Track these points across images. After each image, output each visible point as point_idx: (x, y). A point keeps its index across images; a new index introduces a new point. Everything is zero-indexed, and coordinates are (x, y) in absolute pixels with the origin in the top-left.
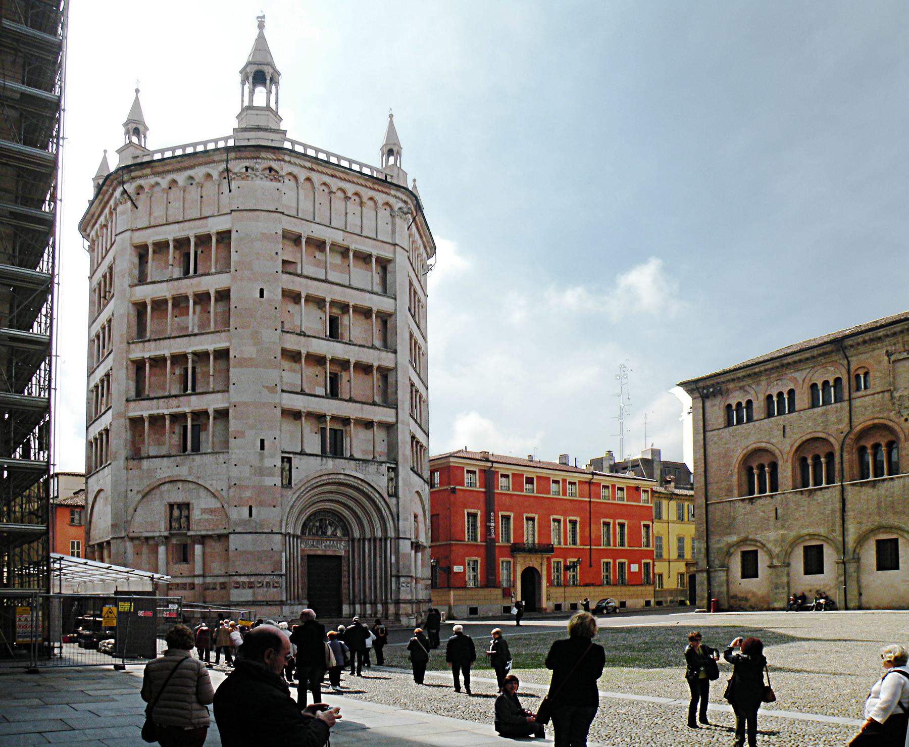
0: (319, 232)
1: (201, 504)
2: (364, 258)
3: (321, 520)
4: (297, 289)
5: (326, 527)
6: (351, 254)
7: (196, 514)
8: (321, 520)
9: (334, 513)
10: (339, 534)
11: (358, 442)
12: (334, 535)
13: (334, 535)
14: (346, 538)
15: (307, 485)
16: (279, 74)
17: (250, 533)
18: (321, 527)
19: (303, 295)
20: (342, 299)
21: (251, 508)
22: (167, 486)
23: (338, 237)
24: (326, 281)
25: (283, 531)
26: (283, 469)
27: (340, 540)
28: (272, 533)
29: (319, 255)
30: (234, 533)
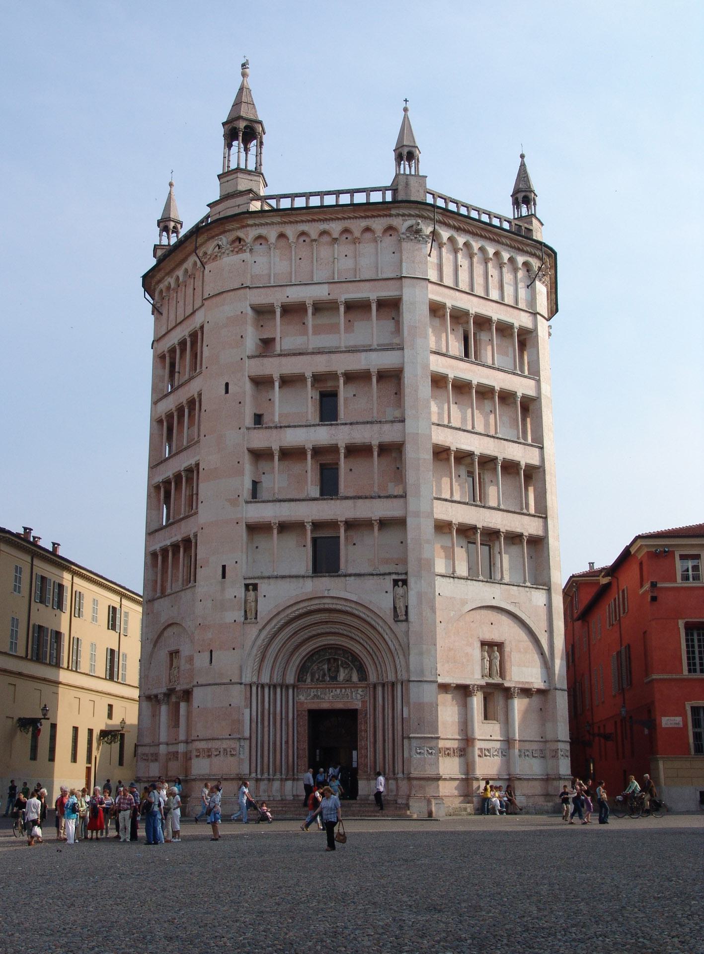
0: (295, 295)
3: (329, 660)
4: (267, 372)
5: (338, 671)
9: (346, 651)
10: (355, 678)
11: (354, 554)
12: (349, 680)
13: (349, 680)
18: (329, 670)
20: (328, 369)
21: (211, 651)
22: (169, 629)
23: (321, 293)
27: (356, 687)
28: (231, 683)
30: (198, 685)
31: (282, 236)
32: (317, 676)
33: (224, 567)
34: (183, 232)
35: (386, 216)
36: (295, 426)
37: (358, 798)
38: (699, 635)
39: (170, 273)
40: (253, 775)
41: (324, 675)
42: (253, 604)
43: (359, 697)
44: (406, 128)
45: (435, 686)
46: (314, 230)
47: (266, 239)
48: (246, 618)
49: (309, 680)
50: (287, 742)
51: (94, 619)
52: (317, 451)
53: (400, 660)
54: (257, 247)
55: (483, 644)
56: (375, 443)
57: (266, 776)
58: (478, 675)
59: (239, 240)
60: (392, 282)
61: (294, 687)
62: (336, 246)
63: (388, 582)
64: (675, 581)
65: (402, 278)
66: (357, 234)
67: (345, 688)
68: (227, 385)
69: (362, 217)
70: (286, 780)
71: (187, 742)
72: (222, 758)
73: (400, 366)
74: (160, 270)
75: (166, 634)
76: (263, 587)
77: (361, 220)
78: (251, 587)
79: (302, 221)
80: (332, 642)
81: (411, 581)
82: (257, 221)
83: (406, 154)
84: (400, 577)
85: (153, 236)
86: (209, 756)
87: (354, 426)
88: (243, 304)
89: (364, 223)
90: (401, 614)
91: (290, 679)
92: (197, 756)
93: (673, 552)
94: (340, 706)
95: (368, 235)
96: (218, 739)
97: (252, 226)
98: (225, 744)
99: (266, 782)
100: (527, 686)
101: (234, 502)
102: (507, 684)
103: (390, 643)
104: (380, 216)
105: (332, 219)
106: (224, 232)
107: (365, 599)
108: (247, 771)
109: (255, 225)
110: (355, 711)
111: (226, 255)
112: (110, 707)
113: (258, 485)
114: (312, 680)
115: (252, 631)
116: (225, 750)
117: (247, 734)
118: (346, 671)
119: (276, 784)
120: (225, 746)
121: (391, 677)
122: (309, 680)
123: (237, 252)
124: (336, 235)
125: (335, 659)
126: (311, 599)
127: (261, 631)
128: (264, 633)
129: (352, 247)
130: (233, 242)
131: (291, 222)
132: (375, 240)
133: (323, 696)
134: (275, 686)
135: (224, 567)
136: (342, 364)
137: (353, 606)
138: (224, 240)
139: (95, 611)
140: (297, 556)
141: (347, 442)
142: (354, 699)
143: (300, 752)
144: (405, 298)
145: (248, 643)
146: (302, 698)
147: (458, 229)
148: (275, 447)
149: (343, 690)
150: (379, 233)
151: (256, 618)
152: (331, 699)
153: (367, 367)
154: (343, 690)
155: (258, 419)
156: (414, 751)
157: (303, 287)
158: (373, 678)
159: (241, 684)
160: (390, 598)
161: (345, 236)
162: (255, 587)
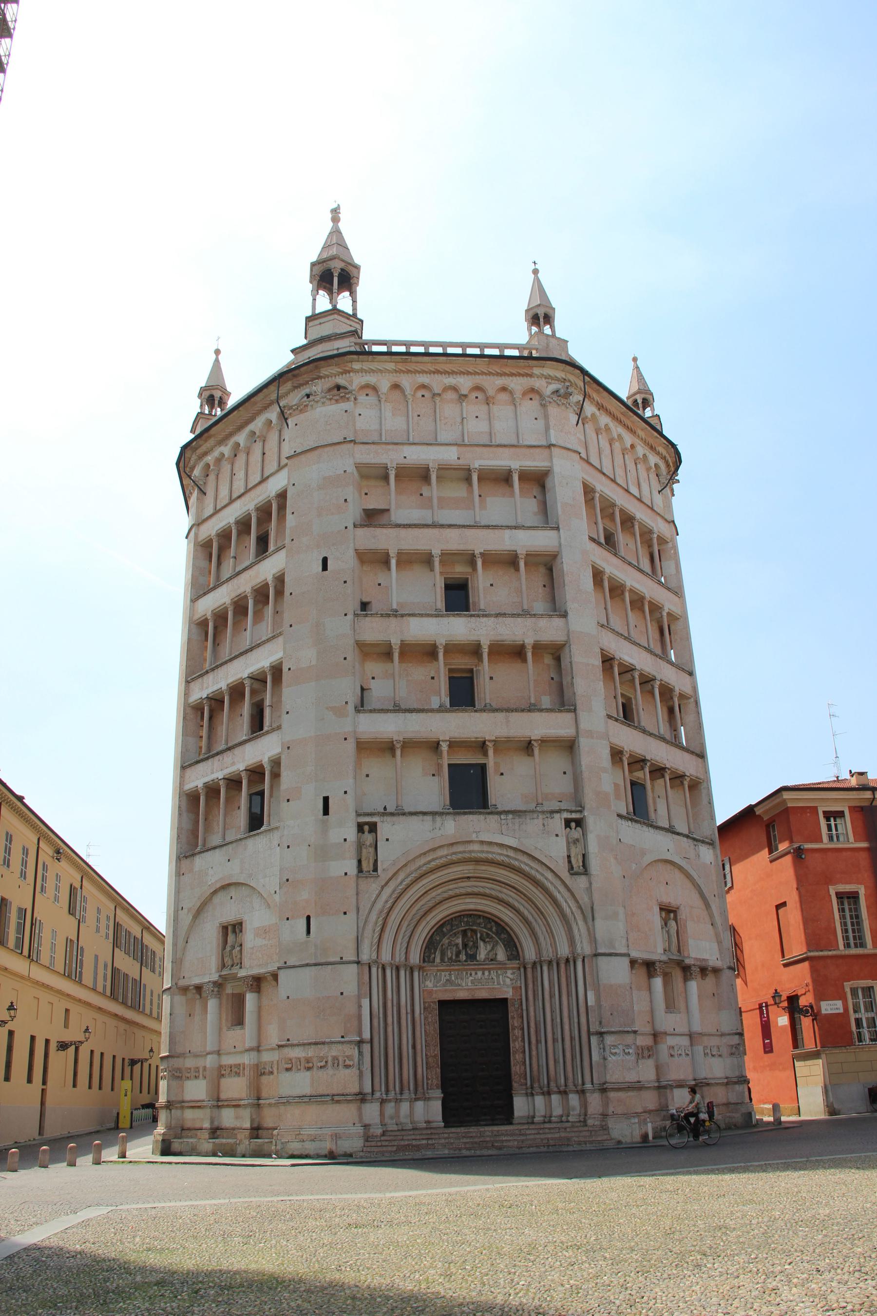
0: (415, 455)
1: (257, 919)
2: (502, 479)
3: (464, 932)
6: (475, 477)
7: (249, 939)
8: (464, 932)
10: (501, 955)
11: (507, 784)
14: (515, 964)
15: (408, 870)
16: (357, 268)
17: (307, 965)
18: (465, 946)
19: (393, 553)
20: (462, 547)
21: (308, 918)
23: (450, 455)
24: (434, 526)
25: (365, 957)
26: (360, 846)
27: (502, 967)
28: (342, 962)
29: (425, 491)
30: (286, 967)
31: (396, 386)
32: (450, 955)
33: (326, 800)
34: (231, 402)
35: (527, 375)
36: (421, 615)
37: (515, 1121)
38: (849, 904)
39: (221, 442)
40: (377, 1095)
41: (458, 954)
42: (372, 850)
43: (508, 980)
44: (538, 288)
45: (626, 961)
46: (437, 382)
47: (375, 389)
48: (360, 870)
49: (438, 960)
50: (414, 1047)
51: (56, 899)
52: (452, 649)
53: (580, 929)
54: (362, 398)
55: (661, 909)
56: (529, 641)
57: (392, 1095)
58: (660, 950)
59: (338, 387)
60: (538, 450)
61: (421, 968)
62: (464, 404)
63: (557, 823)
64: (821, 840)
65: (550, 446)
66: (491, 392)
67: (489, 970)
68: (325, 561)
69: (498, 374)
70: (417, 1099)
71: (218, 1053)
72: (330, 1071)
73: (556, 549)
74: (210, 437)
75: (216, 900)
76: (385, 828)
77: (496, 377)
78: (366, 828)
79: (423, 372)
80: (472, 907)
81: (591, 821)
82: (366, 366)
83: (540, 316)
84: (574, 816)
85: (194, 406)
86: (309, 1069)
87: (501, 619)
88: (343, 462)
89: (500, 382)
90: (581, 867)
91: (415, 958)
92: (287, 1070)
93: (816, 808)
94: (483, 994)
95: (503, 396)
96: (323, 1043)
97: (356, 371)
98: (335, 1051)
99: (393, 1104)
100: (704, 964)
101: (339, 712)
102: (687, 961)
103: (564, 905)
104: (520, 375)
105: (462, 373)
106: (319, 378)
107: (528, 845)
108: (368, 1089)
109: (362, 370)
110: (506, 1000)
111: (320, 404)
112: (67, 1011)
113: (365, 693)
114: (442, 960)
115: (372, 887)
116: (335, 1058)
117: (366, 1035)
118: (489, 947)
119: (405, 1107)
120: (334, 1053)
121: (564, 951)
122: (438, 960)
123: (337, 401)
124: (464, 392)
125: (472, 930)
126: (452, 844)
127: (383, 887)
128: (388, 891)
129: (484, 408)
130: (330, 390)
131: (409, 372)
132: (513, 402)
133: (459, 981)
134: (398, 969)
135: (326, 800)
136: (480, 542)
137: (511, 853)
138: (318, 387)
139: (57, 888)
140: (428, 787)
141: (493, 638)
142: (502, 984)
143: (430, 1060)
144: (557, 469)
145: (365, 905)
146: (429, 984)
147: (600, 407)
148: (395, 642)
149: (487, 973)
150: (518, 395)
151: (375, 869)
152: (470, 985)
153: (513, 548)
155: (364, 606)
156: (607, 1053)
157: (425, 448)
158: (529, 953)
159: (358, 963)
160: (562, 842)
161: (474, 394)
162: (373, 828)
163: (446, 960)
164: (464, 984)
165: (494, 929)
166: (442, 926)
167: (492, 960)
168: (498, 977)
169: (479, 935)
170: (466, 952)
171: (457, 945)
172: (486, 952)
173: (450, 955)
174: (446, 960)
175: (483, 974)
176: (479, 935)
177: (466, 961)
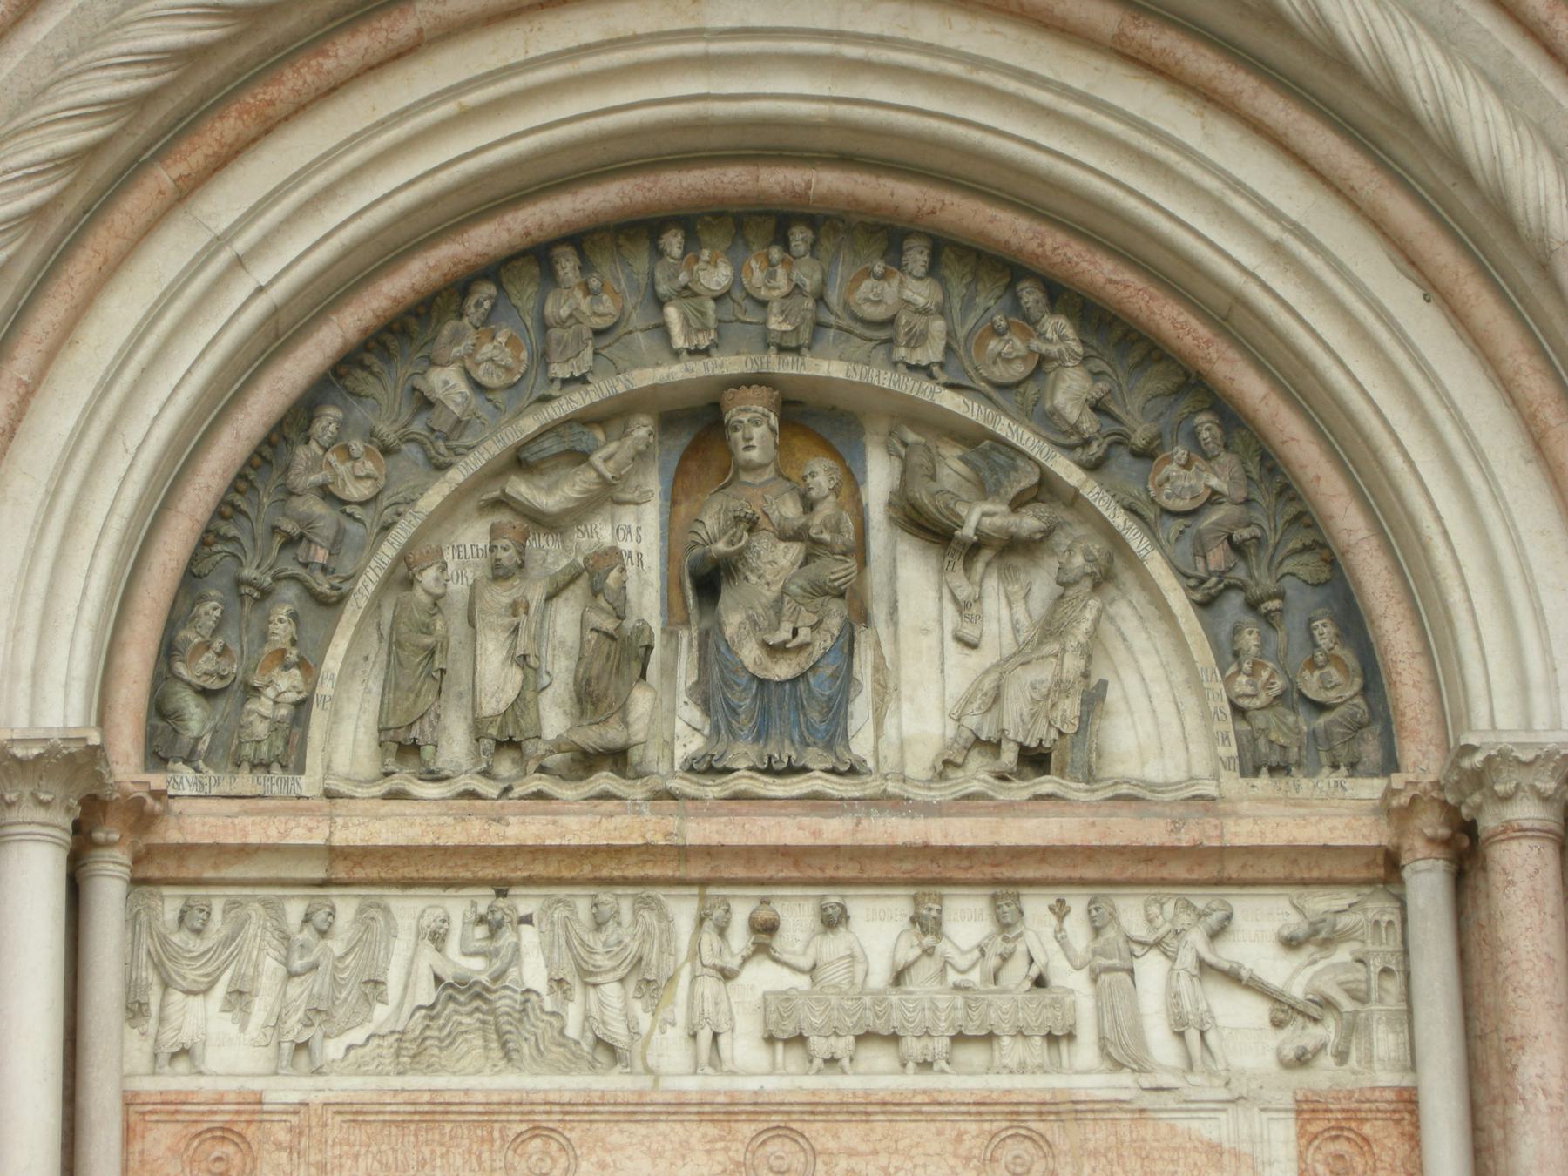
10: (1160, 715)
14: (1335, 810)
18: (708, 581)
32: (496, 678)
41: (619, 657)
43: (1240, 1015)
49: (346, 738)
67: (1002, 874)
114: (404, 747)
122: (346, 738)
125: (811, 419)
154: (967, 920)
163: (454, 745)
164: (670, 1052)
165: (1070, 392)
166: (405, 332)
167: (1035, 760)
168: (1112, 967)
169: (880, 478)
170: (712, 649)
171: (596, 577)
172: (963, 670)
173: (496, 678)
174: (454, 745)
175: (927, 925)
176: (880, 478)
177: (708, 767)
